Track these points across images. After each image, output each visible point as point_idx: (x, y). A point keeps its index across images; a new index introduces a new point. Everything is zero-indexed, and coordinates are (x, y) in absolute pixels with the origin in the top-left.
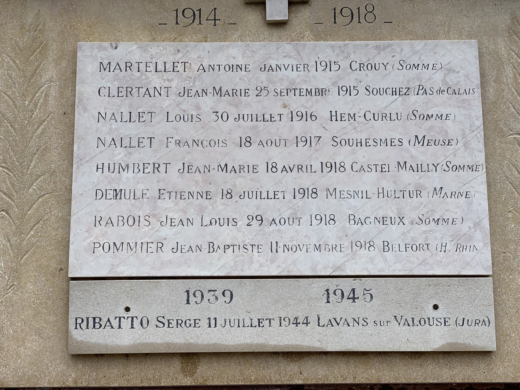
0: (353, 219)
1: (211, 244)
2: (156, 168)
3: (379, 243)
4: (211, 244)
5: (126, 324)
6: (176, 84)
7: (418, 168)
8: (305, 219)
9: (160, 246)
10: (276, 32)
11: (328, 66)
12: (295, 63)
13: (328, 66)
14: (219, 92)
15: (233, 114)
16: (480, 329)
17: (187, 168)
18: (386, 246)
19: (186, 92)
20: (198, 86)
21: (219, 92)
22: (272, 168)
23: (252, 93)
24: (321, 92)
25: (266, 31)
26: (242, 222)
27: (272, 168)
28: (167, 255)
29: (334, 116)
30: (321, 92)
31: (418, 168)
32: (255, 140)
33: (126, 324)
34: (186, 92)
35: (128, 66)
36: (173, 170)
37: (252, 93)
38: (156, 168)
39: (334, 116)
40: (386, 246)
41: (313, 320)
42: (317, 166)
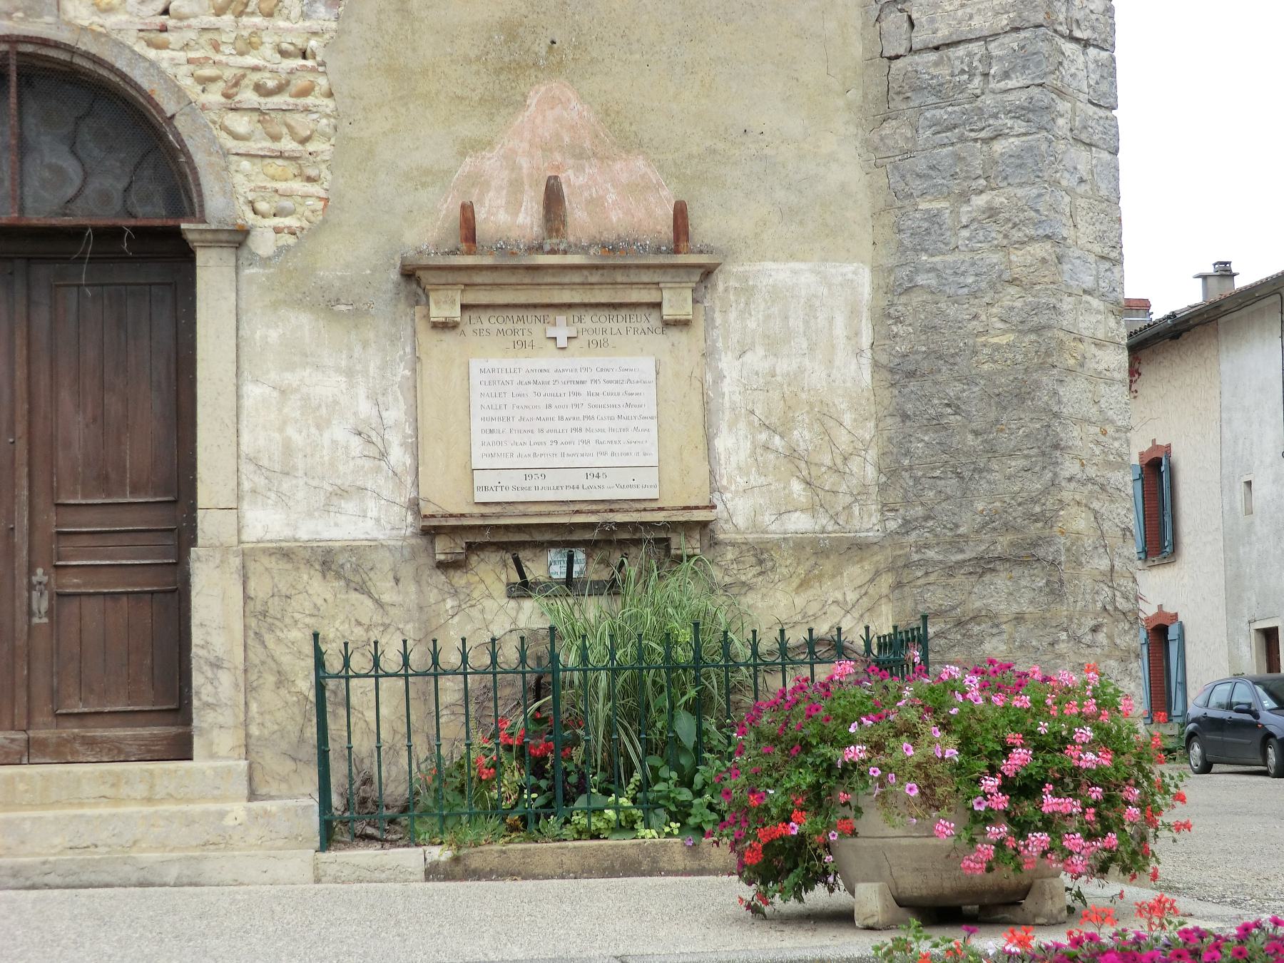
0: (597, 441)
1: (535, 454)
2: (508, 419)
3: (609, 453)
4: (535, 454)
5: (499, 489)
6: (516, 380)
7: (627, 418)
8: (576, 442)
9: (512, 455)
10: (561, 351)
11: (586, 370)
12: (570, 368)
13: (586, 370)
14: (536, 382)
15: (543, 394)
16: (653, 489)
17: (522, 419)
18: (613, 454)
19: (521, 383)
20: (526, 380)
21: (536, 382)
22: (561, 418)
23: (551, 383)
24: (583, 382)
25: (557, 351)
26: (548, 443)
27: (561, 418)
28: (515, 458)
29: (589, 394)
30: (583, 382)
31: (627, 418)
32: (553, 406)
33: (499, 489)
34: (521, 383)
35: (493, 371)
36: (516, 420)
37: (551, 383)
38: (508, 419)
39: (589, 394)
40: (613, 454)
41: (580, 487)
42: (581, 418)
